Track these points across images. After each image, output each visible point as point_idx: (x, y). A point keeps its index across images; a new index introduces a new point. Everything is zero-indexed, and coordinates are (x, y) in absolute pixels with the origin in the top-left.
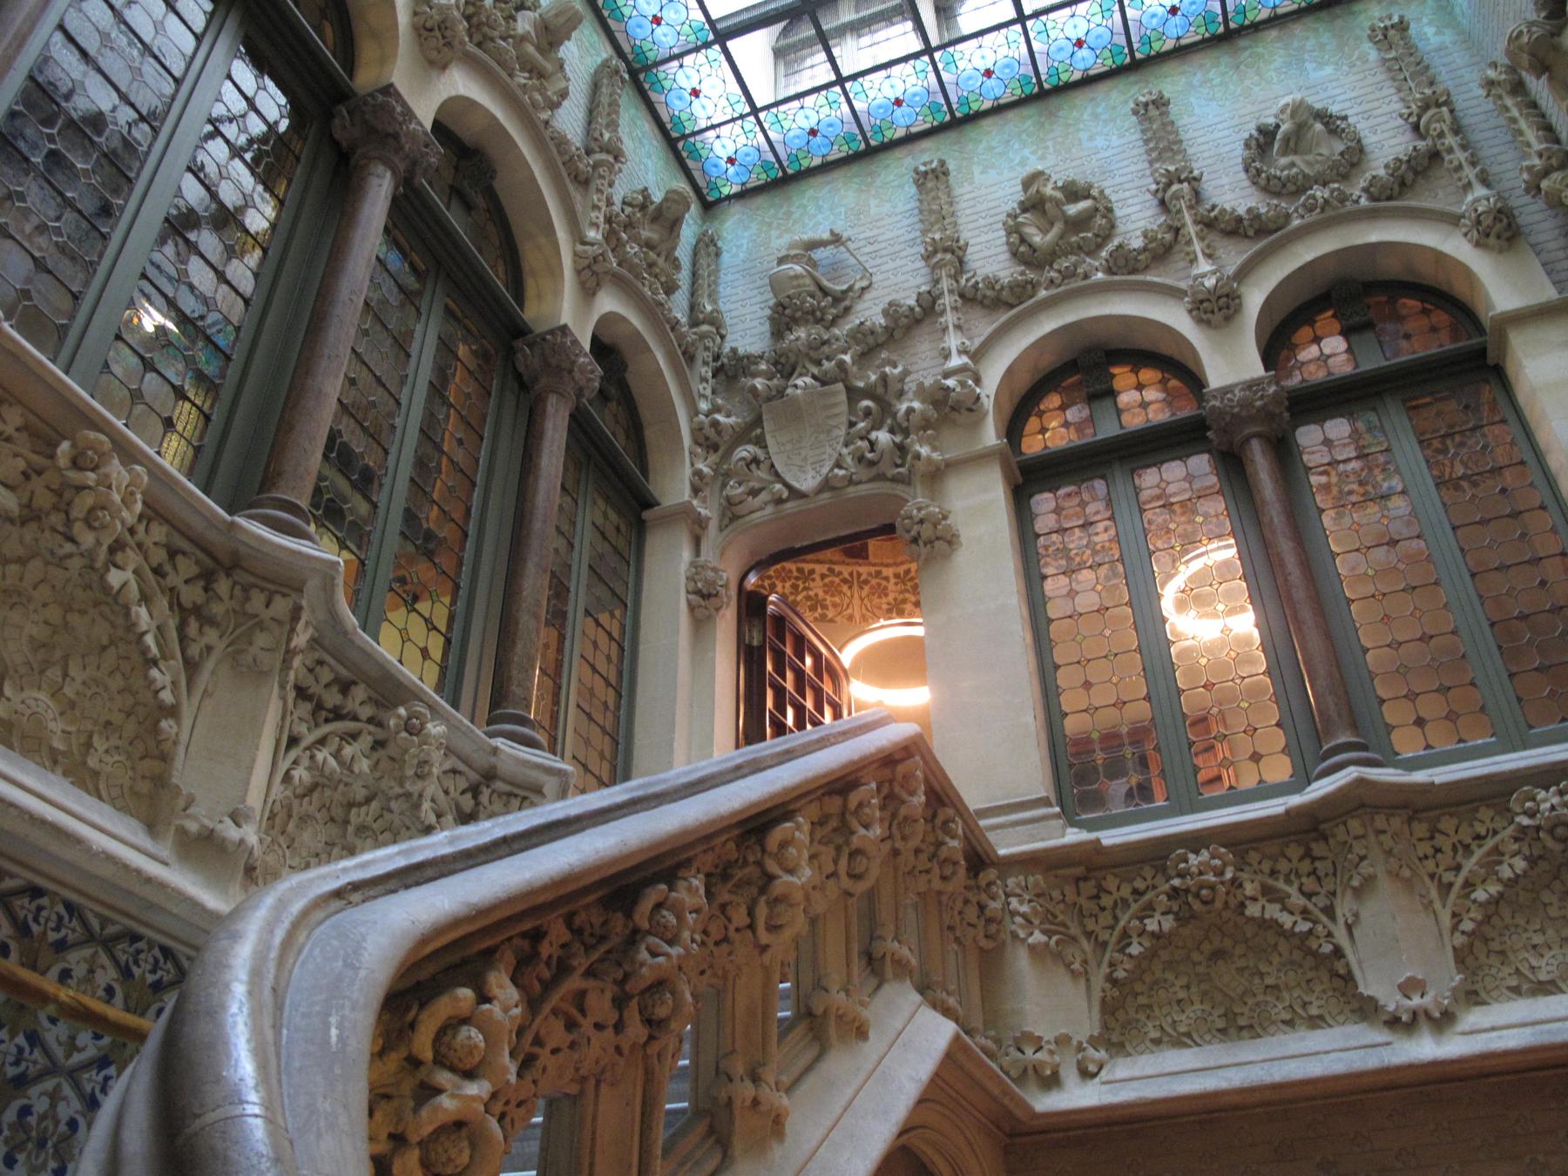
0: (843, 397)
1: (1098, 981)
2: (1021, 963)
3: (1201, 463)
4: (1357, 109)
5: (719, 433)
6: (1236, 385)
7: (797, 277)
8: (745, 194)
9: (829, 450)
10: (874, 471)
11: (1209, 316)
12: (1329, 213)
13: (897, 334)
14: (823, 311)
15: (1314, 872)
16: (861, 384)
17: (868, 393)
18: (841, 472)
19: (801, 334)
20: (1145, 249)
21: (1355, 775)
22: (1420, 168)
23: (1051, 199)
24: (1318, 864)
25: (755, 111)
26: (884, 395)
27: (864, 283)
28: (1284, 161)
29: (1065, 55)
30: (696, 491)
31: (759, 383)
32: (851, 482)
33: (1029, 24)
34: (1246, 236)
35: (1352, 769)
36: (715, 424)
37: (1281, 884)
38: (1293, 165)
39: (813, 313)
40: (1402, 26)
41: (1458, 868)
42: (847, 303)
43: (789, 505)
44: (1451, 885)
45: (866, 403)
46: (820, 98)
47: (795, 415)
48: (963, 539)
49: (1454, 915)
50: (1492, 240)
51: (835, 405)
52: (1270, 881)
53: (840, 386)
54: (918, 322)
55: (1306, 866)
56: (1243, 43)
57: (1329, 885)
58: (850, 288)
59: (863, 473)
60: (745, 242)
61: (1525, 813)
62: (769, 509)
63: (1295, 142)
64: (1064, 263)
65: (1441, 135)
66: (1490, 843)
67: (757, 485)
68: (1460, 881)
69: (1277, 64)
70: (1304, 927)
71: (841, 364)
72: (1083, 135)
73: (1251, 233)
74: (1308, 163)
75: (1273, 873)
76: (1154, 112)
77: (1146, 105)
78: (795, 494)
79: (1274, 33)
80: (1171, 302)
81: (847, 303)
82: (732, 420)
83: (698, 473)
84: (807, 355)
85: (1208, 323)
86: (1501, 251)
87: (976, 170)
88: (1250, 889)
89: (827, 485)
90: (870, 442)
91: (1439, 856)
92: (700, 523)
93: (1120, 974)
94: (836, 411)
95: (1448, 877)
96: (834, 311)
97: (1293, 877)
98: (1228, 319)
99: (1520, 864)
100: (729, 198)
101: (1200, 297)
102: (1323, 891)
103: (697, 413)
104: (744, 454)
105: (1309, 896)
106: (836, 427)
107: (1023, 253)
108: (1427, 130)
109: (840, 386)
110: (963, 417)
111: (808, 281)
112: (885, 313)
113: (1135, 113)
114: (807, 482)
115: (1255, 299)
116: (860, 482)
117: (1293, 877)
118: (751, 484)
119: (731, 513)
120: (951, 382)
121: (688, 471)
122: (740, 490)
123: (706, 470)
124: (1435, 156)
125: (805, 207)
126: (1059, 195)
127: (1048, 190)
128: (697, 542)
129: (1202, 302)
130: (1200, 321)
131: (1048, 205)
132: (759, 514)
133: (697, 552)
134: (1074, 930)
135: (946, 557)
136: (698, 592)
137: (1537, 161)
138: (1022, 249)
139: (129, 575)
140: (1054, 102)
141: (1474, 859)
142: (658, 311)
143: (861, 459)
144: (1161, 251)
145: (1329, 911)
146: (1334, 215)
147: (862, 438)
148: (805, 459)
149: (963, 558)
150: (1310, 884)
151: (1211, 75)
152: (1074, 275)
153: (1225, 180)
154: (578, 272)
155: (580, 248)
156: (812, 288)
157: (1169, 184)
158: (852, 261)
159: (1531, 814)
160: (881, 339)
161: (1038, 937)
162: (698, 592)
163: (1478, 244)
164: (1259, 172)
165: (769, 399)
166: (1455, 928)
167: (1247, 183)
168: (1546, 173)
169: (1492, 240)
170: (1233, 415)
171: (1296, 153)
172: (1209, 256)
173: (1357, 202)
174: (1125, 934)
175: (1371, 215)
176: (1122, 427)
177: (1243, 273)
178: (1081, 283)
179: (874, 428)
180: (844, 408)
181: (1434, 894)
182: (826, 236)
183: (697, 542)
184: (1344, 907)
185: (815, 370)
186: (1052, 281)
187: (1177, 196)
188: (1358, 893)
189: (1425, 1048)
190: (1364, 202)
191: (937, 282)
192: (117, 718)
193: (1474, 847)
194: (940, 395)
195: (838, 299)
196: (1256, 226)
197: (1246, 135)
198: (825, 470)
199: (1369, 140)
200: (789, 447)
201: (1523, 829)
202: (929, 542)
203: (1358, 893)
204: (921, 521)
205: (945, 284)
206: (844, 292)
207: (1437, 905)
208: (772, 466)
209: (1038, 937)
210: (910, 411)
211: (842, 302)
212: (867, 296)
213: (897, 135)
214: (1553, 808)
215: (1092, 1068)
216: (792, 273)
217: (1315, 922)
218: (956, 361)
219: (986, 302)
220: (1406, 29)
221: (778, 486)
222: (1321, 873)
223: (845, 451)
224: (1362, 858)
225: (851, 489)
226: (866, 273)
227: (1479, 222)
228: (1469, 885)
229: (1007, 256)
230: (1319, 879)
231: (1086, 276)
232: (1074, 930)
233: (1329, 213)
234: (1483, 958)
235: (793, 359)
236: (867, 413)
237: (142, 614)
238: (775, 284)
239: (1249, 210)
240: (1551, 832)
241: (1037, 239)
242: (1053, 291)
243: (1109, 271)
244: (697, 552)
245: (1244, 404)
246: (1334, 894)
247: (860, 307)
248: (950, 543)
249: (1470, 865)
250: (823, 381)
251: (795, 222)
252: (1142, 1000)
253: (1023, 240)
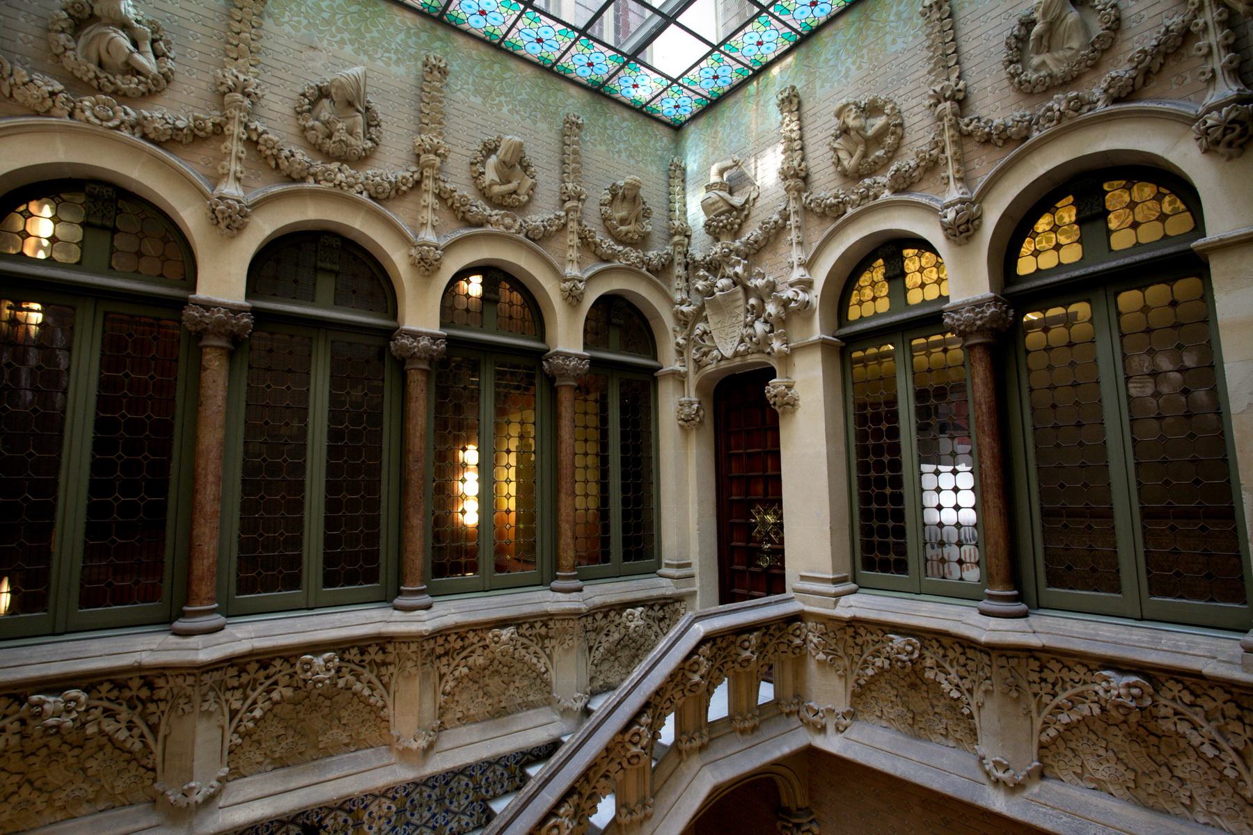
1: (851, 683)
2: (812, 667)
8: (695, 117)
13: (772, 239)
14: (732, 224)
24: (969, 662)
25: (674, 81)
37: (947, 666)
41: (1054, 696)
46: (709, 61)
49: (1045, 723)
52: (941, 662)
68: (1054, 703)
70: (955, 694)
75: (944, 656)
78: (723, 358)
88: (929, 662)
91: (1043, 684)
93: (862, 682)
100: (687, 121)
105: (962, 678)
111: (720, 204)
114: (728, 353)
119: (698, 364)
134: (840, 653)
135: (793, 413)
139: (348, 677)
141: (1066, 695)
145: (970, 691)
149: (800, 414)
150: (962, 671)
155: (563, 285)
161: (821, 656)
166: (1043, 730)
174: (865, 662)
180: (741, 302)
181: (1033, 707)
184: (978, 695)
189: (998, 802)
192: (367, 716)
193: (1068, 686)
207: (1034, 714)
209: (821, 656)
215: (841, 728)
217: (962, 693)
232: (840, 653)
234: (1062, 749)
237: (358, 686)
243: (896, 192)
247: (753, 214)
248: (793, 406)
249: (1062, 698)
252: (874, 694)
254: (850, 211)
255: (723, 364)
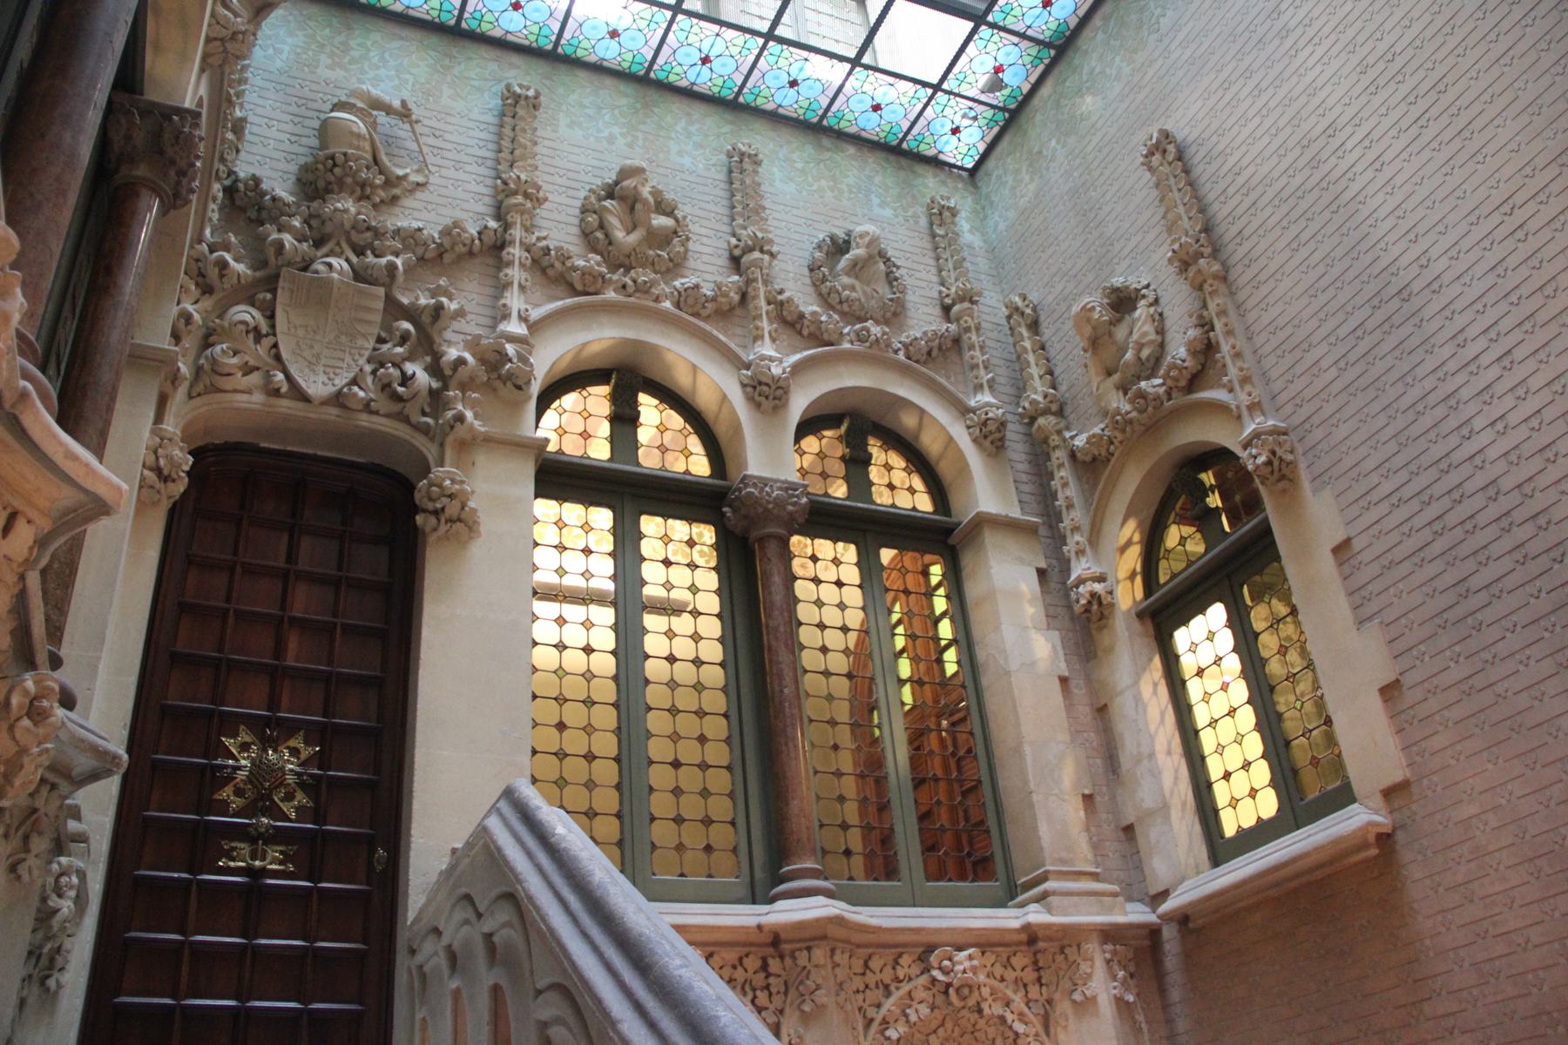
0: (380, 305)
3: (707, 534)
4: (908, 264)
5: (222, 276)
6: (776, 481)
7: (359, 136)
9: (348, 359)
10: (396, 407)
11: (762, 399)
12: (874, 351)
13: (447, 258)
14: (373, 186)
15: (767, 987)
16: (405, 301)
17: (410, 313)
18: (362, 394)
19: (346, 206)
20: (714, 299)
21: (837, 912)
22: (946, 351)
23: (645, 202)
26: (428, 324)
27: (420, 179)
28: (846, 280)
29: (687, 62)
30: (176, 337)
31: (288, 239)
32: (367, 407)
33: (680, 17)
34: (800, 333)
35: (821, 900)
36: (223, 265)
38: (853, 288)
39: (363, 185)
40: (954, 212)
41: (879, 1006)
42: (396, 191)
43: (285, 402)
44: (872, 1020)
45: (407, 325)
47: (320, 295)
48: (482, 529)
50: (987, 443)
51: (369, 310)
53: (381, 291)
54: (471, 254)
55: (759, 979)
56: (826, 142)
57: (778, 1001)
58: (405, 177)
59: (382, 404)
60: (286, 48)
61: (940, 968)
62: (258, 398)
63: (856, 268)
64: (644, 276)
65: (968, 330)
66: (906, 987)
67: (252, 362)
69: (851, 180)
71: (392, 267)
72: (674, 147)
73: (805, 332)
74: (865, 293)
76: (740, 166)
77: (742, 154)
79: (851, 150)
80: (728, 366)
81: (396, 191)
82: (240, 268)
83: (187, 318)
84: (347, 233)
85: (758, 405)
86: (989, 455)
87: (563, 120)
89: (338, 399)
90: (403, 373)
92: (175, 378)
94: (368, 317)
95: (871, 1012)
96: (382, 193)
97: (747, 988)
98: (775, 408)
99: (924, 1010)
101: (764, 379)
102: (772, 1008)
103: (200, 239)
104: (247, 317)
106: (364, 336)
107: (594, 236)
108: (958, 320)
109: (381, 291)
110: (507, 391)
111: (368, 147)
112: (446, 232)
113: (730, 156)
114: (317, 386)
115: (799, 404)
116: (377, 413)
117: (747, 988)
118: (247, 358)
120: (510, 349)
121: (175, 310)
122: (234, 361)
123: (196, 316)
124: (957, 341)
125: (368, 50)
126: (651, 200)
127: (645, 192)
128: (162, 402)
129: (760, 383)
130: (750, 399)
131: (638, 206)
132: (245, 397)
133: (159, 418)
135: (464, 544)
136: (158, 470)
137: (1040, 398)
138: (599, 235)
140: (653, 95)
141: (892, 1000)
142: (224, 105)
143: (386, 387)
144: (726, 308)
146: (875, 354)
147: (394, 365)
148: (318, 356)
149: (478, 550)
151: (795, 156)
152: (647, 292)
153: (790, 268)
154: (209, 40)
156: (369, 157)
157: (751, 250)
158: (414, 146)
159: (946, 972)
160: (429, 255)
162: (158, 470)
163: (975, 440)
164: (824, 279)
165: (289, 264)
167: (808, 281)
168: (1046, 412)
169: (987, 443)
170: (766, 509)
171: (857, 277)
172: (773, 340)
173: (896, 352)
175: (904, 370)
176: (638, 464)
177: (797, 369)
178: (651, 304)
179: (411, 357)
180: (378, 318)
182: (396, 104)
183: (162, 402)
185: (354, 259)
186: (624, 287)
187: (755, 263)
188: (806, 1018)
190: (901, 356)
191: (507, 227)
193: (892, 988)
194: (493, 357)
195: (390, 182)
196: (812, 328)
197: (821, 236)
198: (340, 382)
199: (912, 298)
200: (301, 332)
201: (934, 980)
202: (450, 521)
203: (806, 1018)
204: (451, 496)
205: (517, 233)
206: (399, 178)
208: (275, 346)
210: (461, 362)
211: (393, 190)
212: (419, 195)
213: (492, 33)
214: (964, 972)
216: (355, 129)
218: (515, 327)
219: (550, 272)
220: (954, 215)
221: (280, 376)
222: (774, 990)
223: (368, 368)
224: (818, 987)
225: (364, 416)
226: (423, 167)
227: (985, 423)
228: (885, 1023)
229: (576, 230)
230: (770, 994)
231: (657, 300)
233: (874, 351)
235: (328, 228)
236: (404, 338)
238: (325, 130)
239: (814, 313)
240: (958, 990)
241: (619, 234)
242: (621, 298)
243: (678, 305)
244: (159, 418)
245: (778, 503)
246: (782, 1012)
247: (407, 202)
249: (889, 1004)
250: (359, 275)
251: (353, 61)
253: (602, 226)
254: (611, 295)
255: (286, 406)
